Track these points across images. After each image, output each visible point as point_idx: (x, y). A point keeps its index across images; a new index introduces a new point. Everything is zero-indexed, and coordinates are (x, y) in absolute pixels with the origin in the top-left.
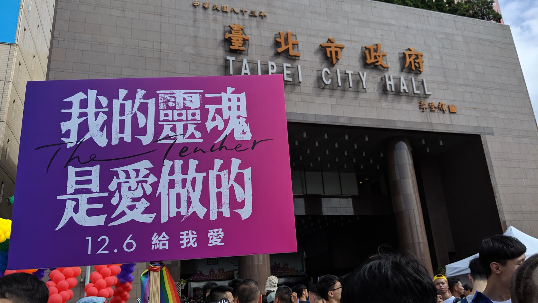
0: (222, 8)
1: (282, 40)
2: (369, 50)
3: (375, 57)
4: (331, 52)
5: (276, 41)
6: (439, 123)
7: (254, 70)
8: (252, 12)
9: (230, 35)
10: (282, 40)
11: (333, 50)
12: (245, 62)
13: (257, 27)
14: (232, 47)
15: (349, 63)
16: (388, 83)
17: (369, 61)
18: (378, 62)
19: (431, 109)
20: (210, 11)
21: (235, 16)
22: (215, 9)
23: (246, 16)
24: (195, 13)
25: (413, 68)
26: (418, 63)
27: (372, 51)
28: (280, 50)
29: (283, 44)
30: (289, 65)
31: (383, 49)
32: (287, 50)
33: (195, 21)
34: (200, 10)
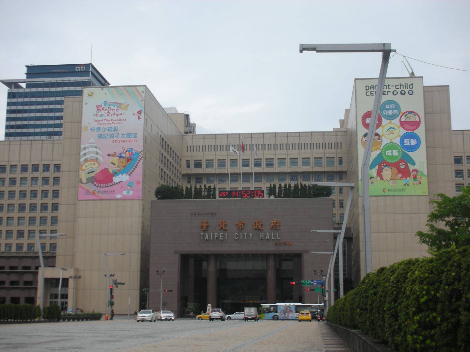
1: (221, 224)
2: (255, 223)
11: (240, 225)
12: (207, 234)
20: (197, 215)
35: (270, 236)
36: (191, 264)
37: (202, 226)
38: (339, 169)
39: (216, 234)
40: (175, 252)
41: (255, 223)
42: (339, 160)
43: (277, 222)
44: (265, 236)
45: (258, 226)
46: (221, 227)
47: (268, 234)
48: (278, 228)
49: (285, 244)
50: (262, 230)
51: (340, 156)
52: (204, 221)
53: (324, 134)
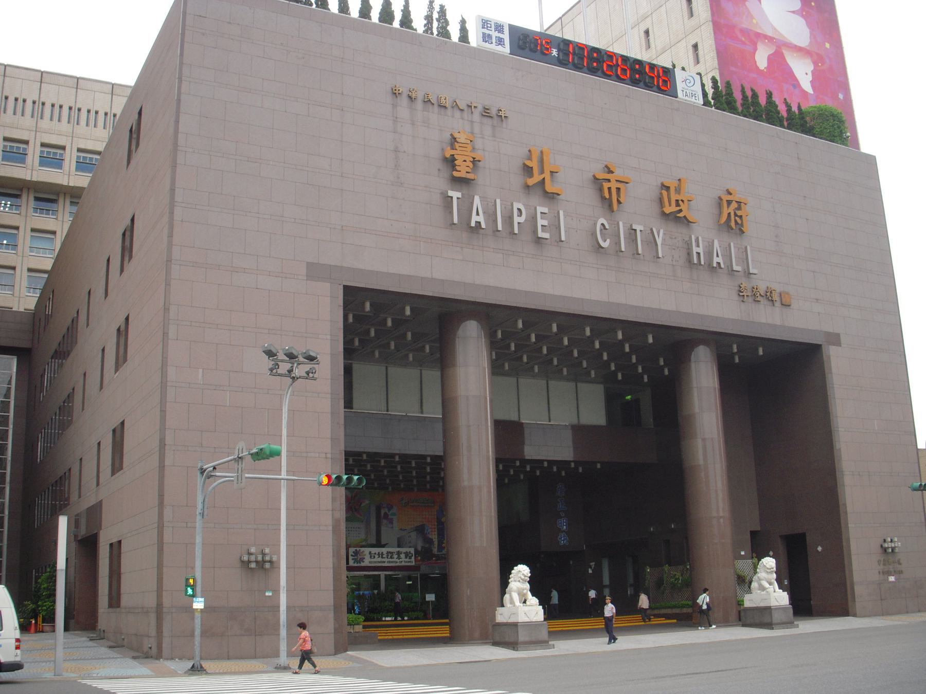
0: (439, 99)
2: (668, 188)
3: (678, 205)
4: (609, 189)
5: (525, 165)
6: (767, 321)
7: (491, 216)
8: (486, 109)
9: (453, 152)
10: (534, 164)
11: (614, 185)
12: (477, 201)
13: (494, 136)
14: (456, 174)
15: (638, 212)
16: (695, 250)
17: (668, 210)
18: (681, 211)
19: (755, 296)
20: (419, 105)
21: (458, 114)
22: (427, 102)
23: (476, 116)
24: (394, 106)
25: (733, 224)
26: (741, 217)
27: (672, 190)
28: (531, 182)
30: (546, 210)
31: (690, 189)
32: (543, 182)
33: (395, 120)
34: (404, 100)
40: (315, 271)
46: (537, 178)
49: (769, 296)
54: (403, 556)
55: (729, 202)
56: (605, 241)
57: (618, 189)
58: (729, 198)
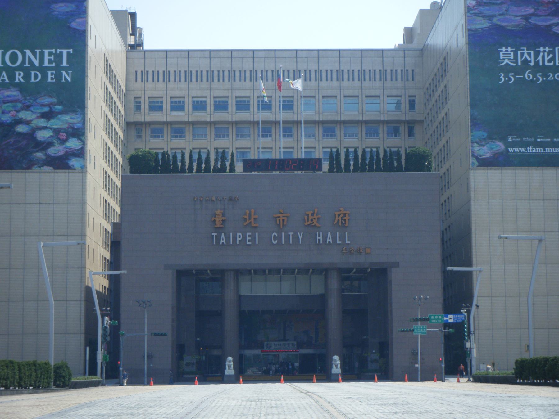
1: (247, 217)
2: (308, 215)
4: (279, 220)
11: (281, 219)
12: (223, 235)
16: (318, 238)
17: (307, 223)
26: (345, 220)
27: (310, 215)
28: (245, 224)
29: (248, 219)
30: (250, 234)
35: (334, 238)
36: (197, 286)
37: (215, 221)
38: (409, 116)
39: (238, 234)
41: (308, 215)
42: (410, 101)
43: (345, 215)
44: (325, 238)
45: (312, 220)
46: (248, 222)
47: (329, 234)
48: (346, 225)
49: (358, 251)
50: (319, 227)
51: (412, 93)
52: (218, 212)
53: (382, 52)
54: (291, 345)
55: (339, 215)
56: (275, 241)
57: (283, 220)
58: (340, 213)
